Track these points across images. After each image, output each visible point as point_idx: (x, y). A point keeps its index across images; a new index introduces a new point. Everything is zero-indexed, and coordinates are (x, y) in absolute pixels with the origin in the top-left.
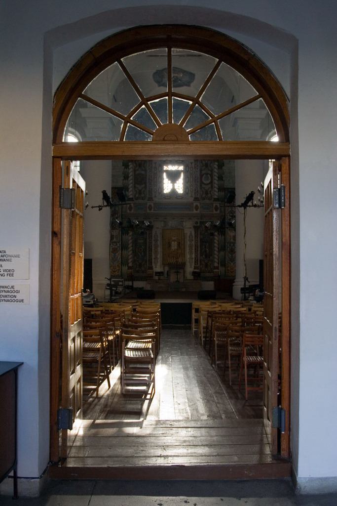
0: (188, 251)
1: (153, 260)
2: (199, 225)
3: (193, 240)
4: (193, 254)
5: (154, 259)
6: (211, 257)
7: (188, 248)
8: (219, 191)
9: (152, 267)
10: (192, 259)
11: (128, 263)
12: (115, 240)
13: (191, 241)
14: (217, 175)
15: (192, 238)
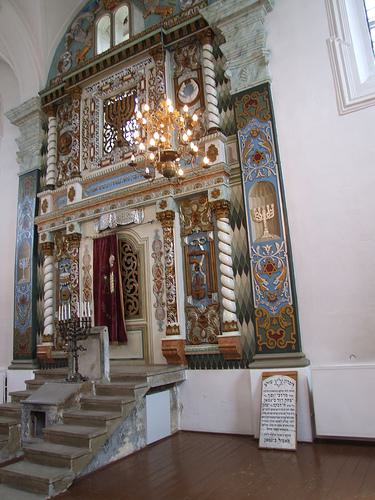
0: (152, 283)
3: (161, 253)
6: (215, 296)
7: (152, 278)
8: (220, 112)
11: (43, 328)
12: (22, 281)
13: (157, 255)
14: (212, 74)
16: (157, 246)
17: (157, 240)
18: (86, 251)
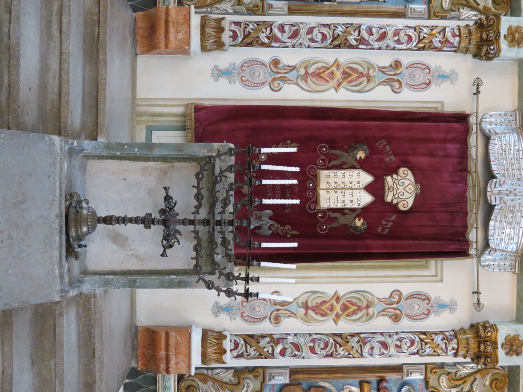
1: (264, 55)
2: (504, 360)
3: (396, 318)
4: (306, 318)
5: (276, 62)
7: (343, 289)
9: (220, 45)
10: (277, 320)
13: (394, 307)
15: (411, 317)
16: (418, 307)
17: (429, 304)
18: (446, 83)
